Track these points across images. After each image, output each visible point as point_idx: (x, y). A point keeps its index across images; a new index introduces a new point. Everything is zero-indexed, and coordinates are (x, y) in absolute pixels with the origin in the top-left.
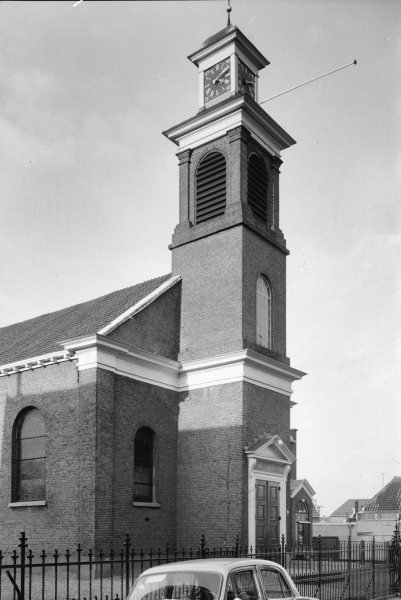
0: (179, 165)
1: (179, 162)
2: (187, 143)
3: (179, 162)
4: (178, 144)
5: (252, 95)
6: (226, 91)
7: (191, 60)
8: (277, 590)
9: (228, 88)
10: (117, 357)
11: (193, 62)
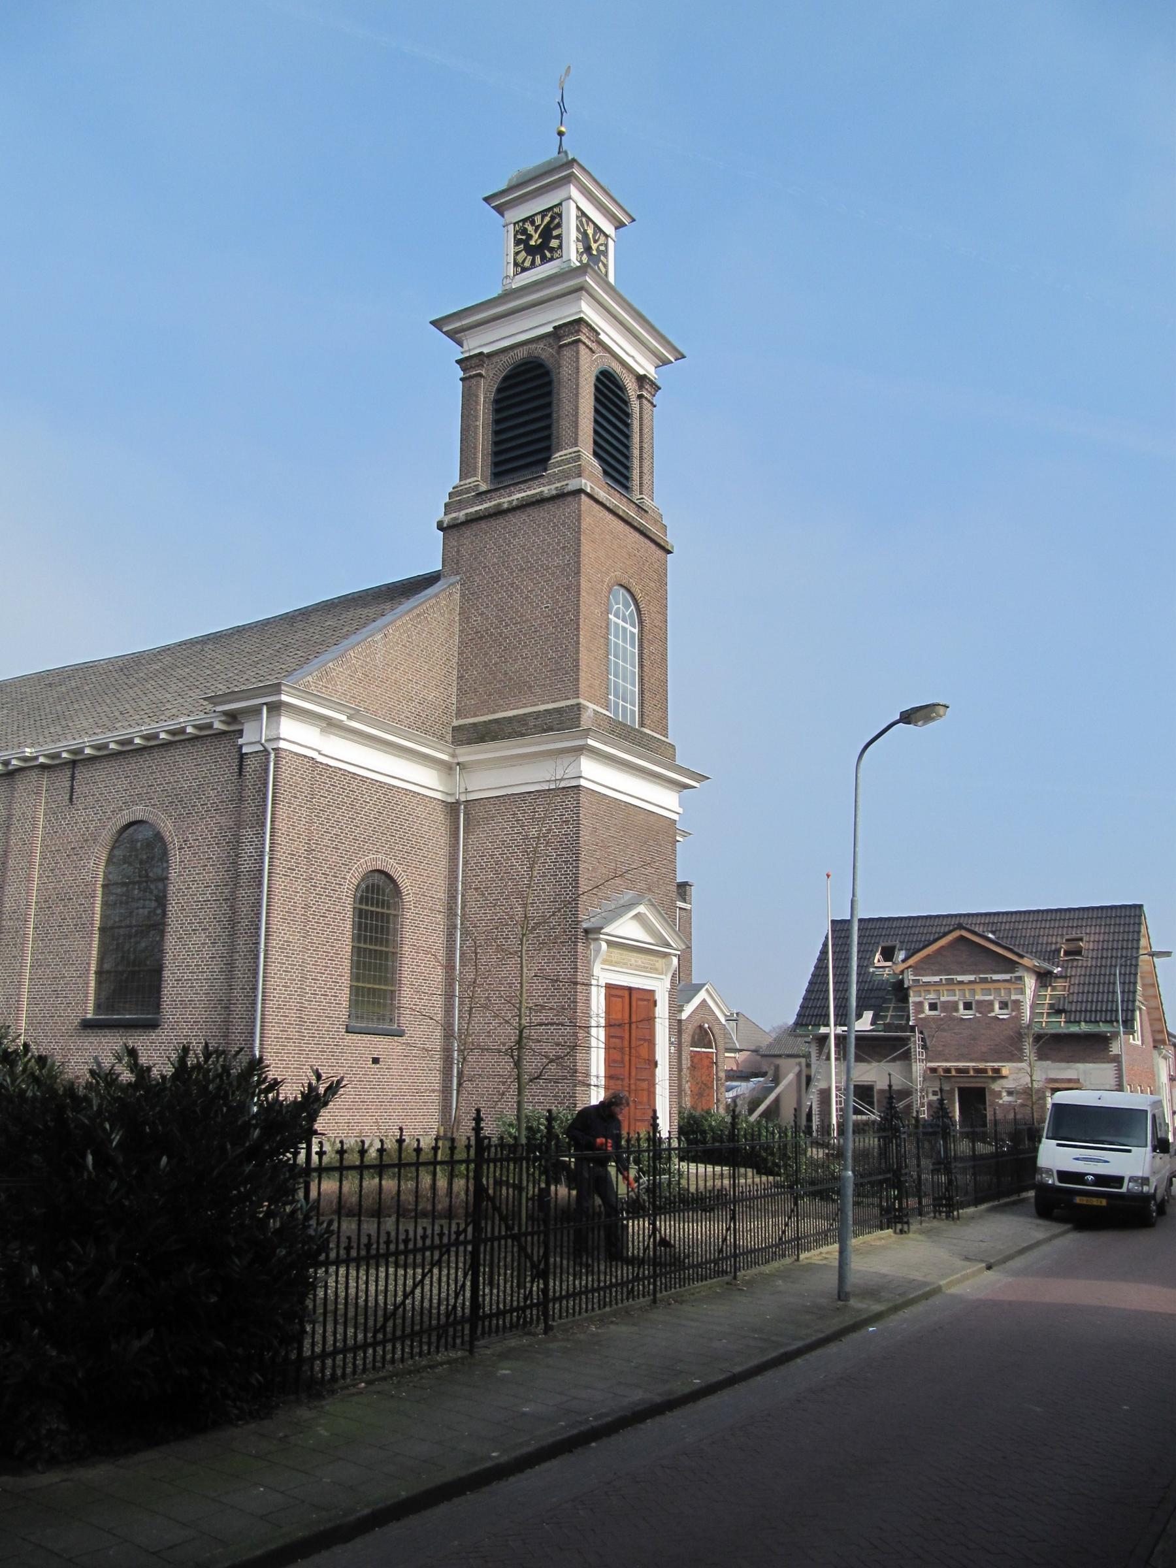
0: (462, 379)
1: (461, 374)
2: (482, 342)
3: (461, 374)
4: (460, 344)
5: (603, 270)
6: (552, 259)
7: (490, 205)
8: (718, 1169)
9: (556, 255)
10: (323, 730)
11: (492, 207)
